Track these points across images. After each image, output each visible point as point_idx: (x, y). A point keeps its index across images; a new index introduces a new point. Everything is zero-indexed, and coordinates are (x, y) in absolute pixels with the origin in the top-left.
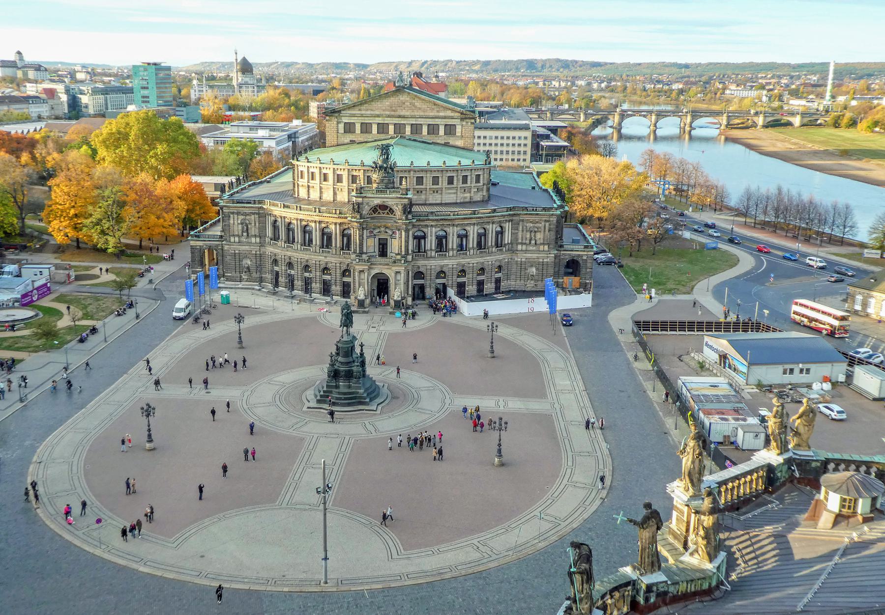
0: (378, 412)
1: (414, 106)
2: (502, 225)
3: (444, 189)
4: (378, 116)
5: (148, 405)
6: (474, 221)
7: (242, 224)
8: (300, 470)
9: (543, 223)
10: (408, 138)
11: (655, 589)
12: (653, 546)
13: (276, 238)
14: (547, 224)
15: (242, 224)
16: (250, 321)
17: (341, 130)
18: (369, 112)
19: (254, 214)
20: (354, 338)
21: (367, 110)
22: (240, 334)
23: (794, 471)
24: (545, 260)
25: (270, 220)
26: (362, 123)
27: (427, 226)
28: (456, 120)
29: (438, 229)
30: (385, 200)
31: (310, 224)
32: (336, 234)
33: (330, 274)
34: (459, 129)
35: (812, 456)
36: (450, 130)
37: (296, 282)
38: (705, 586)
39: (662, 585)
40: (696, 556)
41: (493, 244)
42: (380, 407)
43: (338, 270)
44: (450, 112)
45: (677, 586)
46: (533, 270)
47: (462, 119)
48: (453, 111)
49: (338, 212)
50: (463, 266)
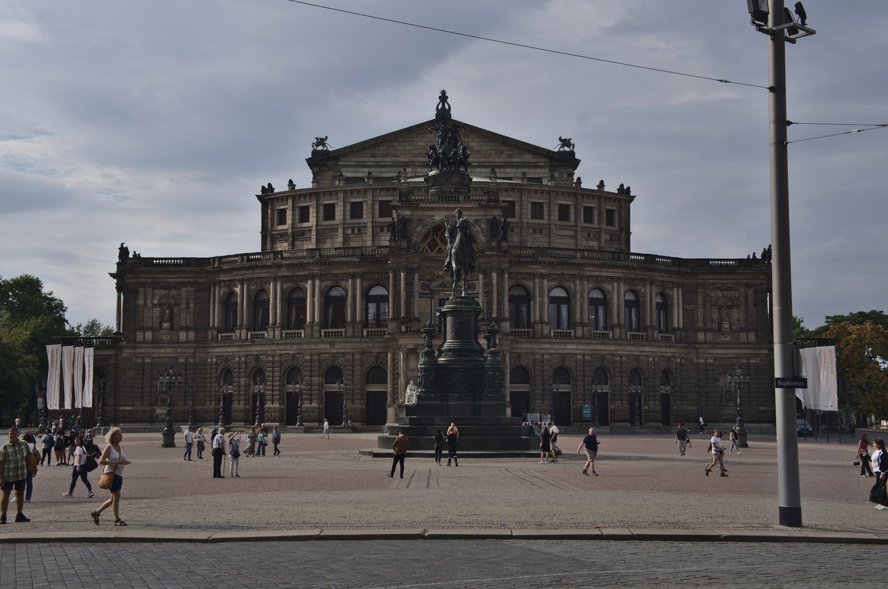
2: (667, 291)
3: (553, 226)
7: (160, 305)
9: (742, 290)
13: (228, 325)
14: (751, 292)
15: (160, 305)
21: (386, 156)
25: (218, 293)
27: (532, 276)
28: (543, 170)
29: (554, 283)
31: (301, 284)
32: (354, 296)
41: (654, 324)
43: (358, 368)
47: (552, 169)
50: (603, 358)
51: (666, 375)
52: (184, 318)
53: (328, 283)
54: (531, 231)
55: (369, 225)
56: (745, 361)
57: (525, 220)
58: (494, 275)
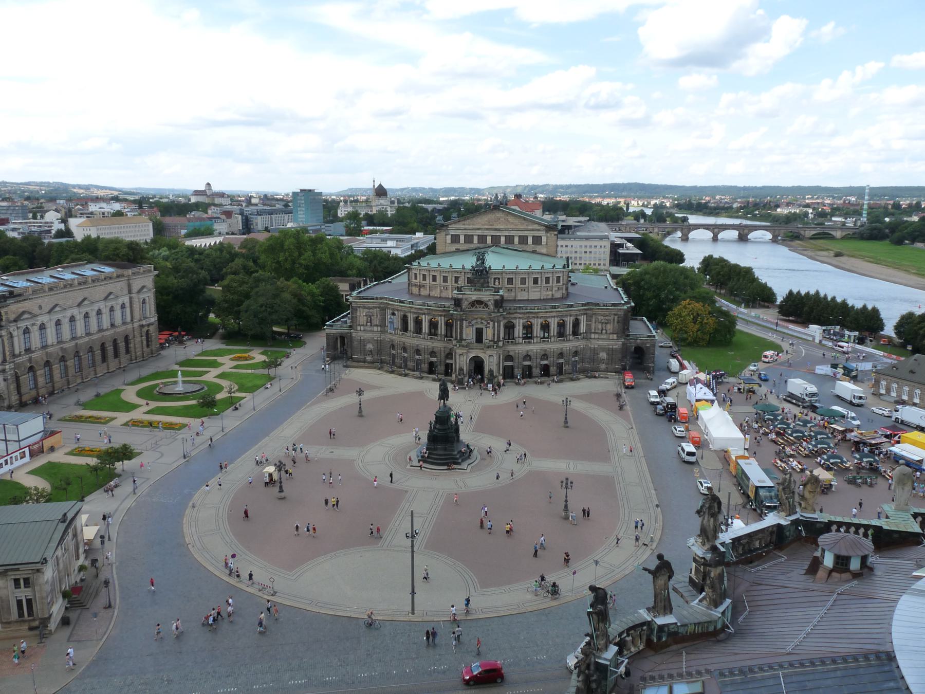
0: (468, 470)
1: (508, 221)
2: (578, 317)
4: (478, 229)
5: (280, 462)
6: (554, 314)
7: (366, 315)
8: (401, 518)
10: (502, 246)
11: (666, 629)
12: (665, 592)
14: (616, 317)
15: (366, 315)
16: (366, 396)
17: (449, 241)
18: (471, 226)
19: (376, 308)
20: (450, 409)
21: (469, 225)
22: (360, 404)
23: (801, 530)
24: (614, 347)
26: (465, 235)
27: (515, 318)
30: (481, 296)
33: (436, 357)
34: (544, 239)
35: (817, 519)
36: (537, 240)
37: (408, 363)
38: (711, 629)
39: (672, 626)
40: (705, 602)
42: (470, 467)
44: (537, 225)
45: (686, 627)
46: (603, 355)
47: (547, 232)
48: (539, 224)
49: (443, 306)
50: (545, 350)
51: (576, 353)
52: (376, 321)
53: (431, 317)
54: (520, 290)
55: (450, 287)
56: (611, 347)
57: (517, 286)
58: (496, 324)
